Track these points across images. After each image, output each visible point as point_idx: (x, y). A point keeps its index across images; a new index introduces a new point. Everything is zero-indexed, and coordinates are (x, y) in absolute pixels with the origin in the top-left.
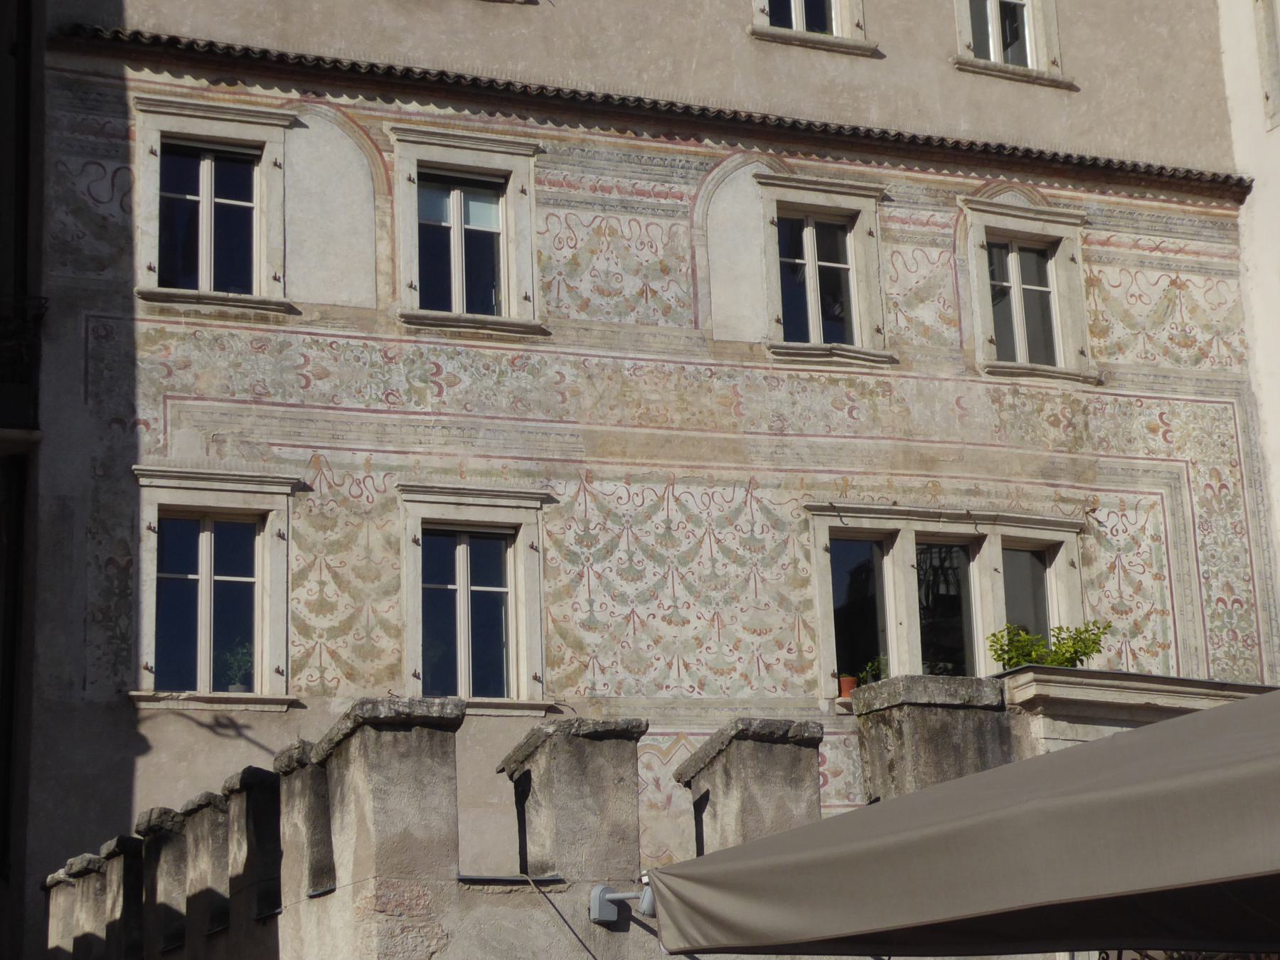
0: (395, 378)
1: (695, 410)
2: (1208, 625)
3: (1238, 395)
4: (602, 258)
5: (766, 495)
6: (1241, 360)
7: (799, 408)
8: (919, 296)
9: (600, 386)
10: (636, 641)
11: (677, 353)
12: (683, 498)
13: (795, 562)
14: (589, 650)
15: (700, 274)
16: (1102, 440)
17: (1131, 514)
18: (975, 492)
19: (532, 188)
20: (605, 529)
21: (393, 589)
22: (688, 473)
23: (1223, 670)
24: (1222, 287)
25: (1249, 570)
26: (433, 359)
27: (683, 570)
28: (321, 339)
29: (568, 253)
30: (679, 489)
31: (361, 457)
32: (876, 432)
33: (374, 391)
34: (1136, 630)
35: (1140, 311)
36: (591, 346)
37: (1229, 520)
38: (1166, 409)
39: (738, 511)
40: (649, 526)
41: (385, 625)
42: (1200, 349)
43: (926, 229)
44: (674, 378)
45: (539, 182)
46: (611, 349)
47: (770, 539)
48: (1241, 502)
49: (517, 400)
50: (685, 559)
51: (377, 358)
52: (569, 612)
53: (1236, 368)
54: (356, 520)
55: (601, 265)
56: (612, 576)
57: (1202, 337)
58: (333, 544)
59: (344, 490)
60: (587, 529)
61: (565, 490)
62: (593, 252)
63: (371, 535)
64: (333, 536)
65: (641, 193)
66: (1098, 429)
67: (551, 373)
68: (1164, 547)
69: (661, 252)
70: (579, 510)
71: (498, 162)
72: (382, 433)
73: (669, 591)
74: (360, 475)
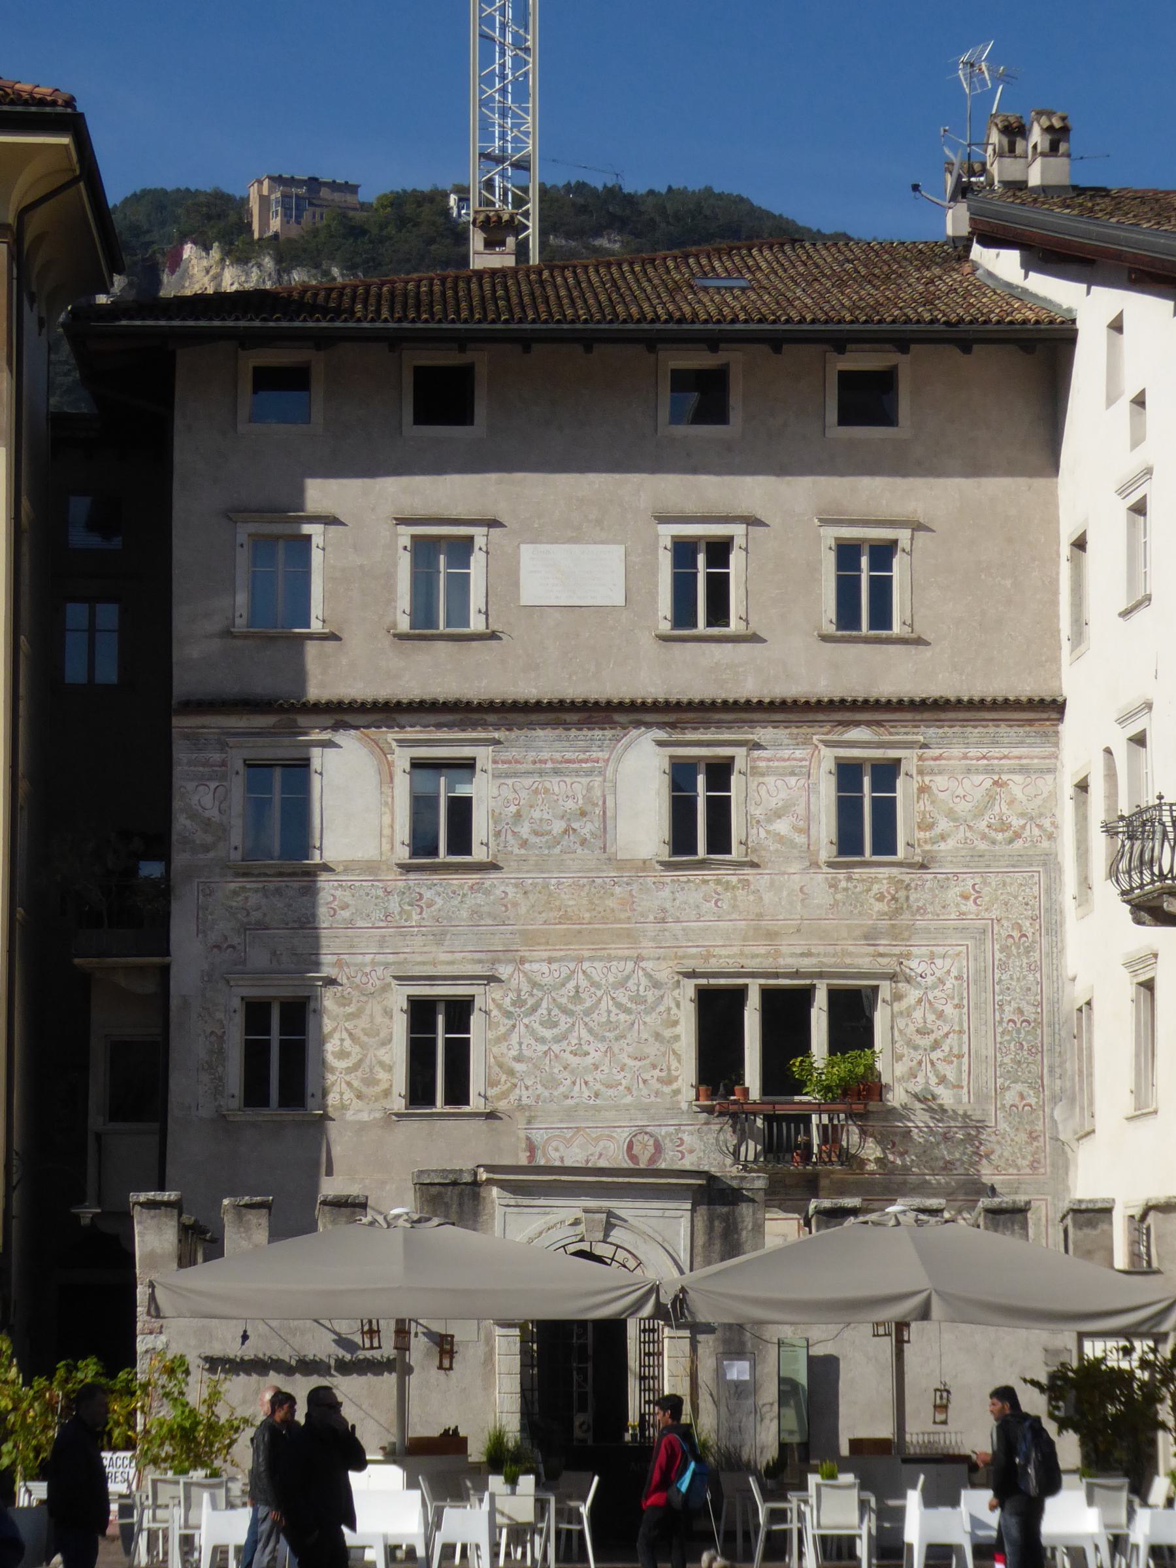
0: (392, 905)
1: (601, 909)
2: (999, 1039)
3: (1045, 864)
4: (538, 809)
5: (648, 965)
6: (1050, 837)
7: (677, 902)
8: (778, 814)
9: (532, 898)
10: (551, 1067)
11: (591, 870)
12: (588, 971)
13: (669, 1009)
14: (518, 1075)
15: (608, 814)
16: (919, 908)
17: (939, 962)
18: (809, 954)
19: (490, 767)
20: (532, 995)
21: (388, 1041)
22: (593, 953)
23: (1008, 1072)
24: (1040, 782)
25: (1039, 997)
26: (417, 890)
27: (587, 1019)
28: (344, 884)
29: (513, 809)
30: (586, 965)
31: (368, 958)
32: (734, 916)
33: (378, 914)
34: (936, 1045)
35: (962, 807)
36: (528, 872)
37: (1025, 961)
38: (978, 880)
39: (628, 977)
40: (563, 991)
41: (381, 1064)
42: (1015, 832)
43: (787, 763)
44: (587, 888)
45: (495, 762)
46: (542, 872)
47: (651, 995)
48: (1037, 946)
49: (474, 912)
50: (588, 1012)
51: (380, 893)
52: (505, 1051)
53: (1045, 844)
54: (364, 999)
55: (536, 814)
56: (536, 1026)
57: (1016, 822)
58: (350, 1014)
59: (357, 980)
60: (519, 995)
61: (504, 971)
62: (531, 807)
63: (374, 1007)
64: (349, 1010)
65: (569, 761)
66: (918, 900)
67: (498, 892)
68: (965, 985)
69: (581, 802)
70: (514, 983)
71: (466, 752)
72: (382, 941)
73: (576, 1034)
74: (368, 970)
